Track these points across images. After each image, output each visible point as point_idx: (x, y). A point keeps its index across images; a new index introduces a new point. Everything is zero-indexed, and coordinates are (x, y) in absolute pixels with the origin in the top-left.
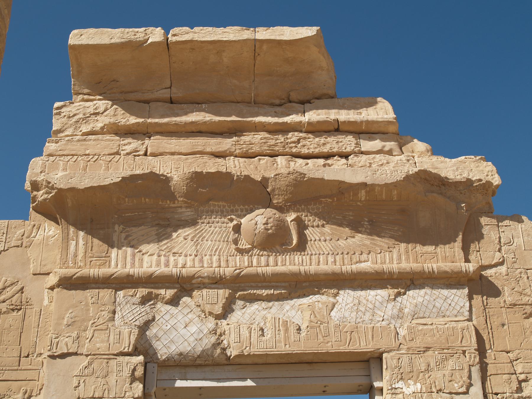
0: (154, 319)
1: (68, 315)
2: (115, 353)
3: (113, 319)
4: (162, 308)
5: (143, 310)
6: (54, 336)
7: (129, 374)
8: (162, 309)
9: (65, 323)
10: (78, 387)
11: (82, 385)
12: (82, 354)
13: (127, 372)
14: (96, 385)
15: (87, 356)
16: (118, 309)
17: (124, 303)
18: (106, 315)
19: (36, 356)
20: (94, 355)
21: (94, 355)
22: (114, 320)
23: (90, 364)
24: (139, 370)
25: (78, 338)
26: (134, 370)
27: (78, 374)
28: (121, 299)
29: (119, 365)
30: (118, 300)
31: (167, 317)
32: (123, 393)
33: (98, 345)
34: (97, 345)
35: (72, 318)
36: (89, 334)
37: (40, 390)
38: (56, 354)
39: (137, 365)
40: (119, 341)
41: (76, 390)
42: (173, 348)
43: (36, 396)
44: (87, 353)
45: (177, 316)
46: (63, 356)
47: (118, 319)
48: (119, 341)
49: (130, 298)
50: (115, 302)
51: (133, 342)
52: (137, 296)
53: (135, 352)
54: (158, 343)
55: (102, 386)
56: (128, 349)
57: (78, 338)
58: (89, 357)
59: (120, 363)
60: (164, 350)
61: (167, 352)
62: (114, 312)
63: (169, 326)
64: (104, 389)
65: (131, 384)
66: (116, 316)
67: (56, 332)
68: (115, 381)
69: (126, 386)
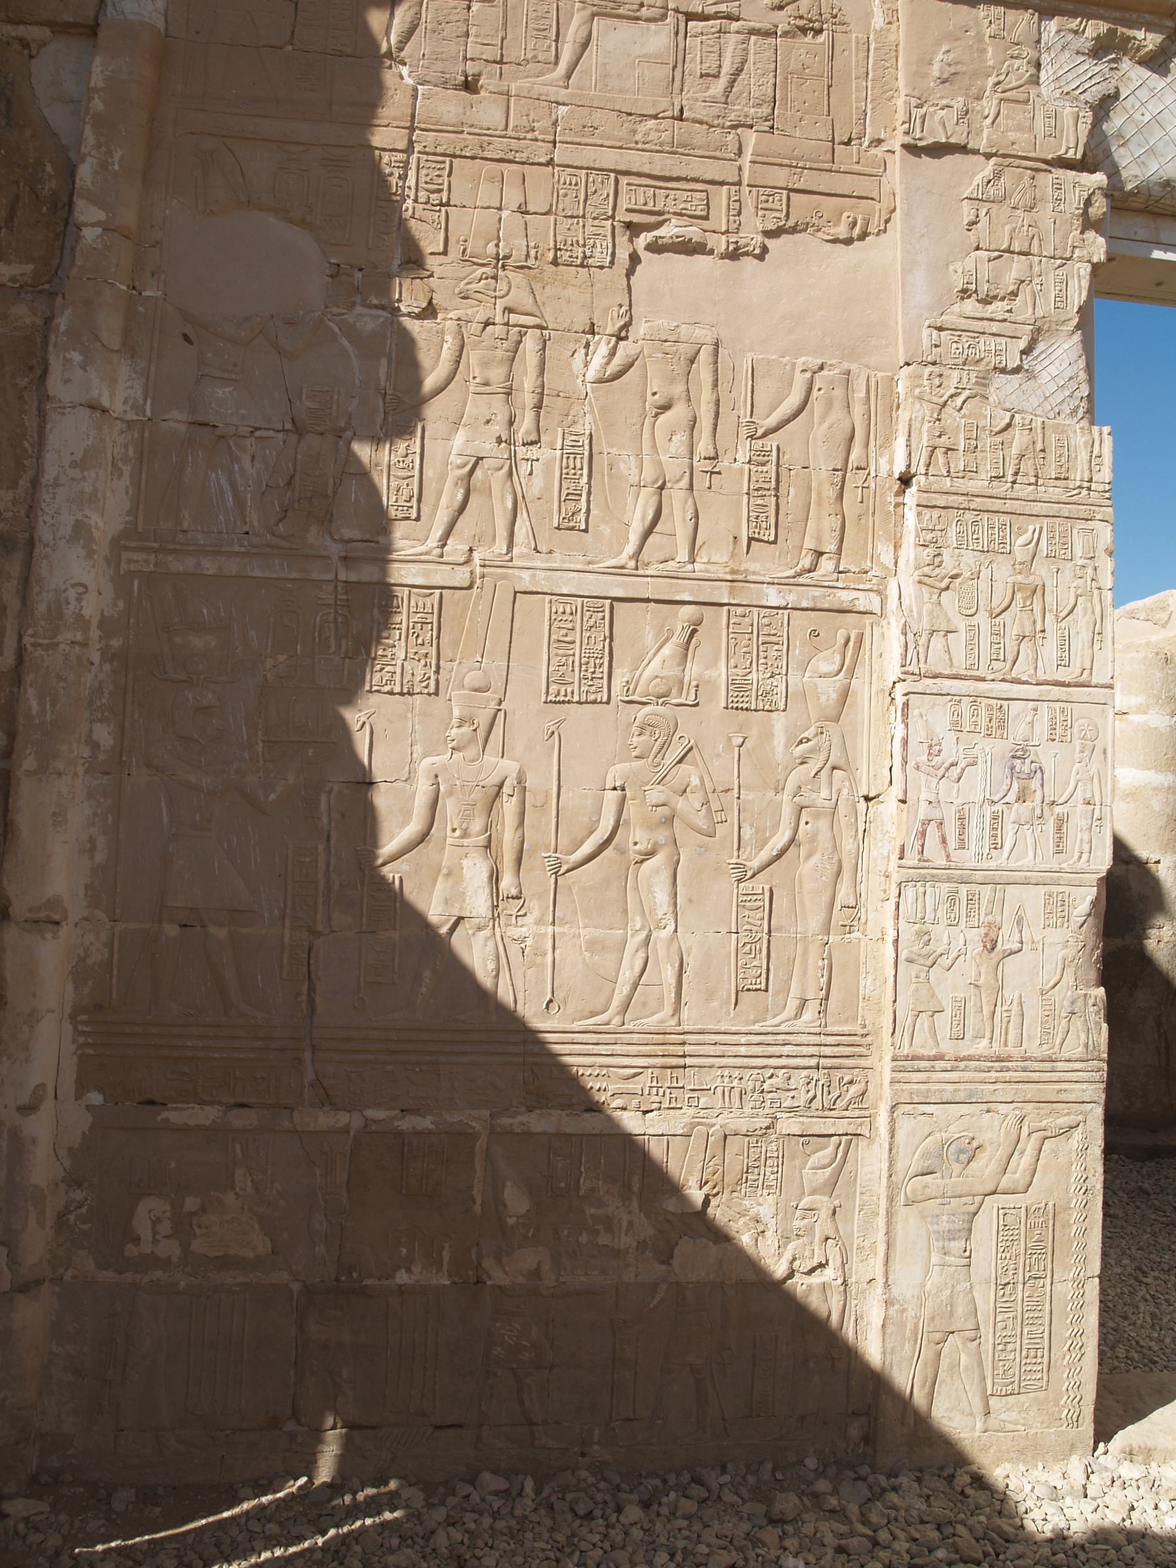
0: (1116, 96)
1: (940, 56)
2: (1049, 157)
3: (1035, 81)
4: (1133, 74)
5: (1097, 69)
6: (914, 102)
7: (1078, 209)
8: (1132, 74)
9: (936, 73)
10: (976, 223)
11: (984, 220)
12: (976, 152)
13: (1075, 206)
14: (1014, 225)
15: (988, 156)
16: (1045, 59)
17: (1059, 46)
18: (1023, 68)
19: (866, 143)
20: (1004, 156)
21: (1004, 156)
22: (1038, 84)
23: (997, 175)
24: (1097, 204)
25: (967, 112)
26: (1088, 203)
27: (974, 196)
28: (1051, 35)
29: (1058, 186)
30: (1044, 37)
31: (1143, 94)
32: (1069, 249)
33: (1012, 136)
34: (1009, 134)
35: (950, 65)
36: (989, 105)
37: (887, 221)
38: (920, 144)
39: (1094, 192)
40: (1055, 133)
41: (970, 230)
42: (1153, 167)
43: (878, 234)
44: (988, 150)
45: (1162, 95)
46: (938, 150)
47: (1047, 83)
48: (1055, 133)
49: (1071, 36)
50: (1039, 41)
51: (1083, 139)
52: (1086, 35)
53: (1084, 165)
54: (1122, 151)
55: (1025, 228)
56: (1076, 154)
57: (967, 112)
58: (994, 160)
59: (1059, 181)
60: (1135, 170)
61: (1139, 173)
62: (1038, 66)
63: (1147, 117)
64: (1030, 234)
65: (1082, 232)
66: (1043, 75)
67: (916, 93)
68: (1052, 220)
69: (1074, 236)
